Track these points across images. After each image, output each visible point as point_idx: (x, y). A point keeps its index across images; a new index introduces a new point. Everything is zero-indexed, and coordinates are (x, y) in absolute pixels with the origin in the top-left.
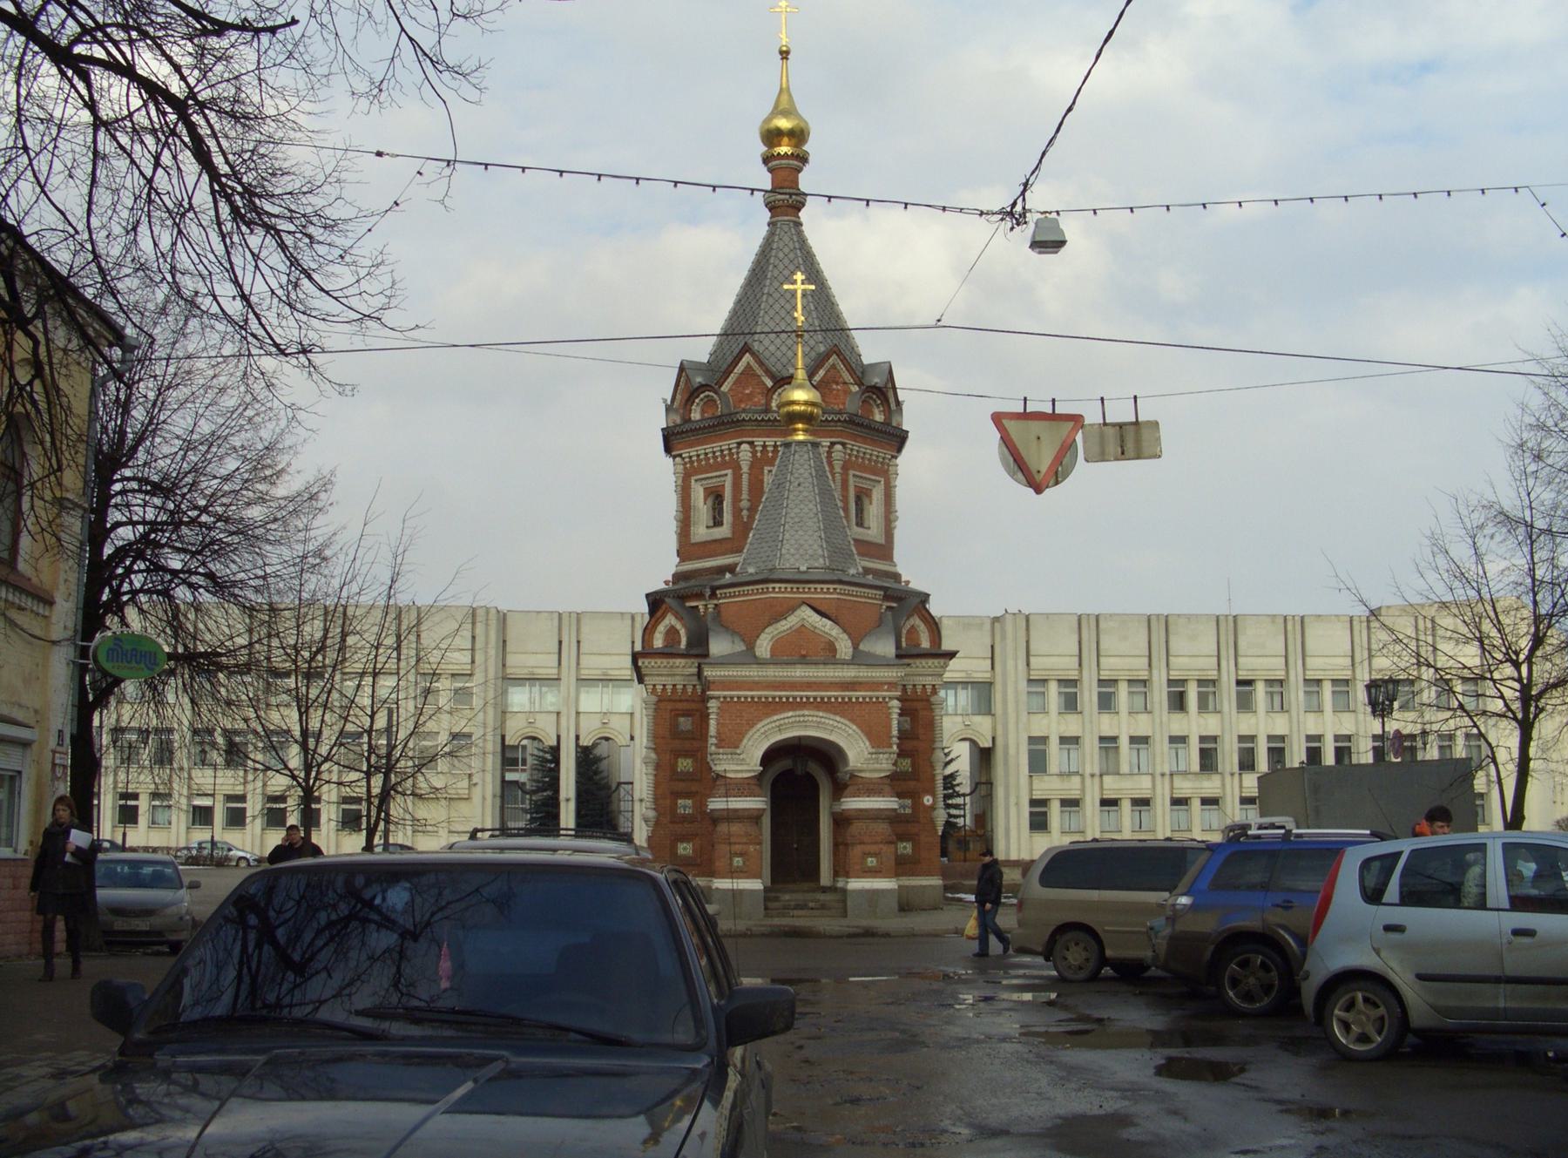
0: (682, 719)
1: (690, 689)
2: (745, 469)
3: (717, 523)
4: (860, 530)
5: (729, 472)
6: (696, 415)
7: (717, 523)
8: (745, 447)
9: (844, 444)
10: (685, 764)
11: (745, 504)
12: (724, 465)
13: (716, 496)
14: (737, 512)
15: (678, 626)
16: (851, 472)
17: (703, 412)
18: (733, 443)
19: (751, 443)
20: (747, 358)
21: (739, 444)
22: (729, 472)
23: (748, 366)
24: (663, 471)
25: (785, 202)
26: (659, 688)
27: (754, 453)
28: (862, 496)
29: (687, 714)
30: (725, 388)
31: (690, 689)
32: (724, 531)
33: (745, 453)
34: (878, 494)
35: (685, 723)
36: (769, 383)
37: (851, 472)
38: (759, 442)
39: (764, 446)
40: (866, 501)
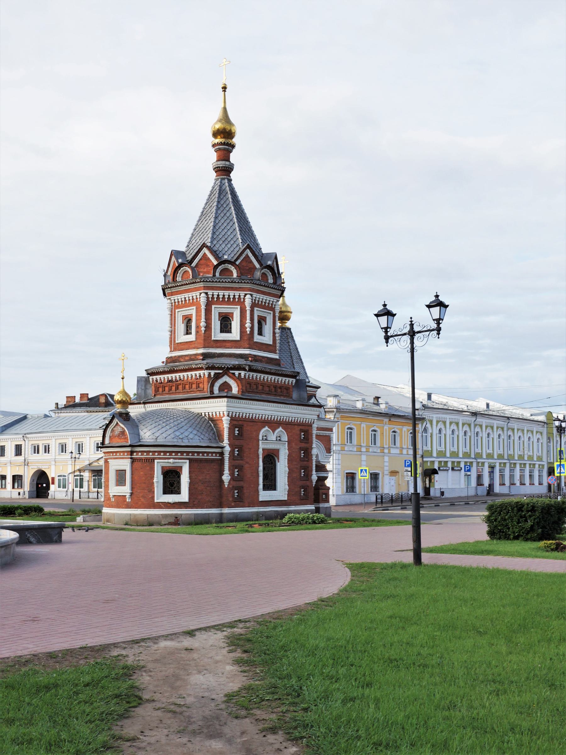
2: (203, 307)
5: (194, 307)
6: (179, 279)
7: (188, 332)
9: (251, 295)
11: (203, 324)
12: (192, 304)
13: (188, 320)
14: (198, 327)
16: (256, 309)
18: (198, 293)
19: (206, 293)
20: (205, 250)
21: (201, 293)
22: (194, 307)
24: (164, 305)
27: (208, 298)
28: (262, 321)
30: (194, 264)
32: (192, 337)
33: (203, 300)
36: (215, 263)
37: (256, 309)
38: (210, 293)
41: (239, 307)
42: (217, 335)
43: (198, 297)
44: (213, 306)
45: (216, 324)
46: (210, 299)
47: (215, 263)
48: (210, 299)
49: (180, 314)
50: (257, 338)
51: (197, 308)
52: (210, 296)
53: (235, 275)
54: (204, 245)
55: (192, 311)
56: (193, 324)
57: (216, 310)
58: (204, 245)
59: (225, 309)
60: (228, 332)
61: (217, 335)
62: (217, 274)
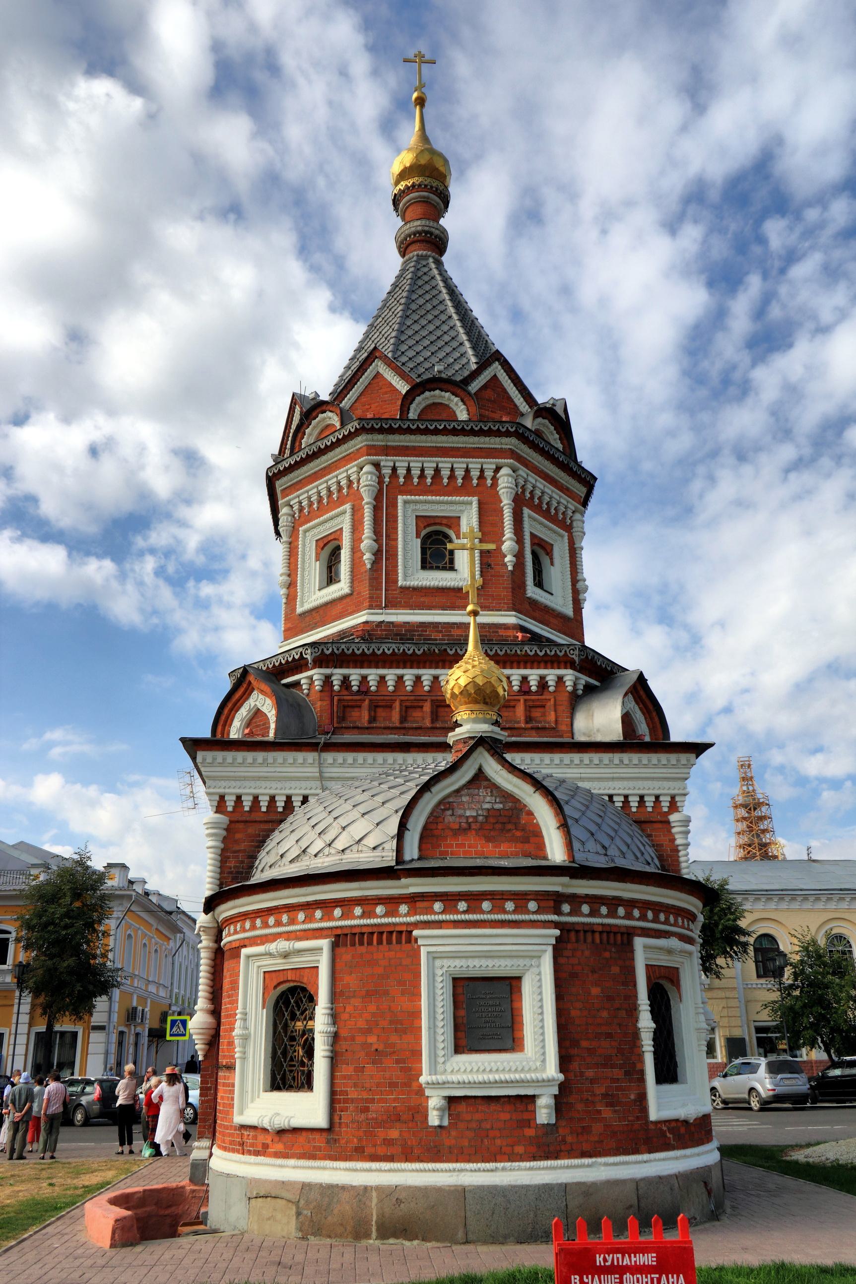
3: (331, 577)
4: (538, 590)
5: (347, 507)
7: (331, 577)
8: (367, 468)
34: (561, 550)
40: (545, 560)
41: (475, 500)
42: (412, 574)
44: (400, 499)
45: (408, 547)
47: (403, 387)
49: (309, 539)
50: (532, 591)
53: (462, 415)
55: (341, 521)
56: (345, 555)
57: (407, 510)
59: (436, 506)
60: (444, 569)
61: (412, 574)
62: (412, 415)
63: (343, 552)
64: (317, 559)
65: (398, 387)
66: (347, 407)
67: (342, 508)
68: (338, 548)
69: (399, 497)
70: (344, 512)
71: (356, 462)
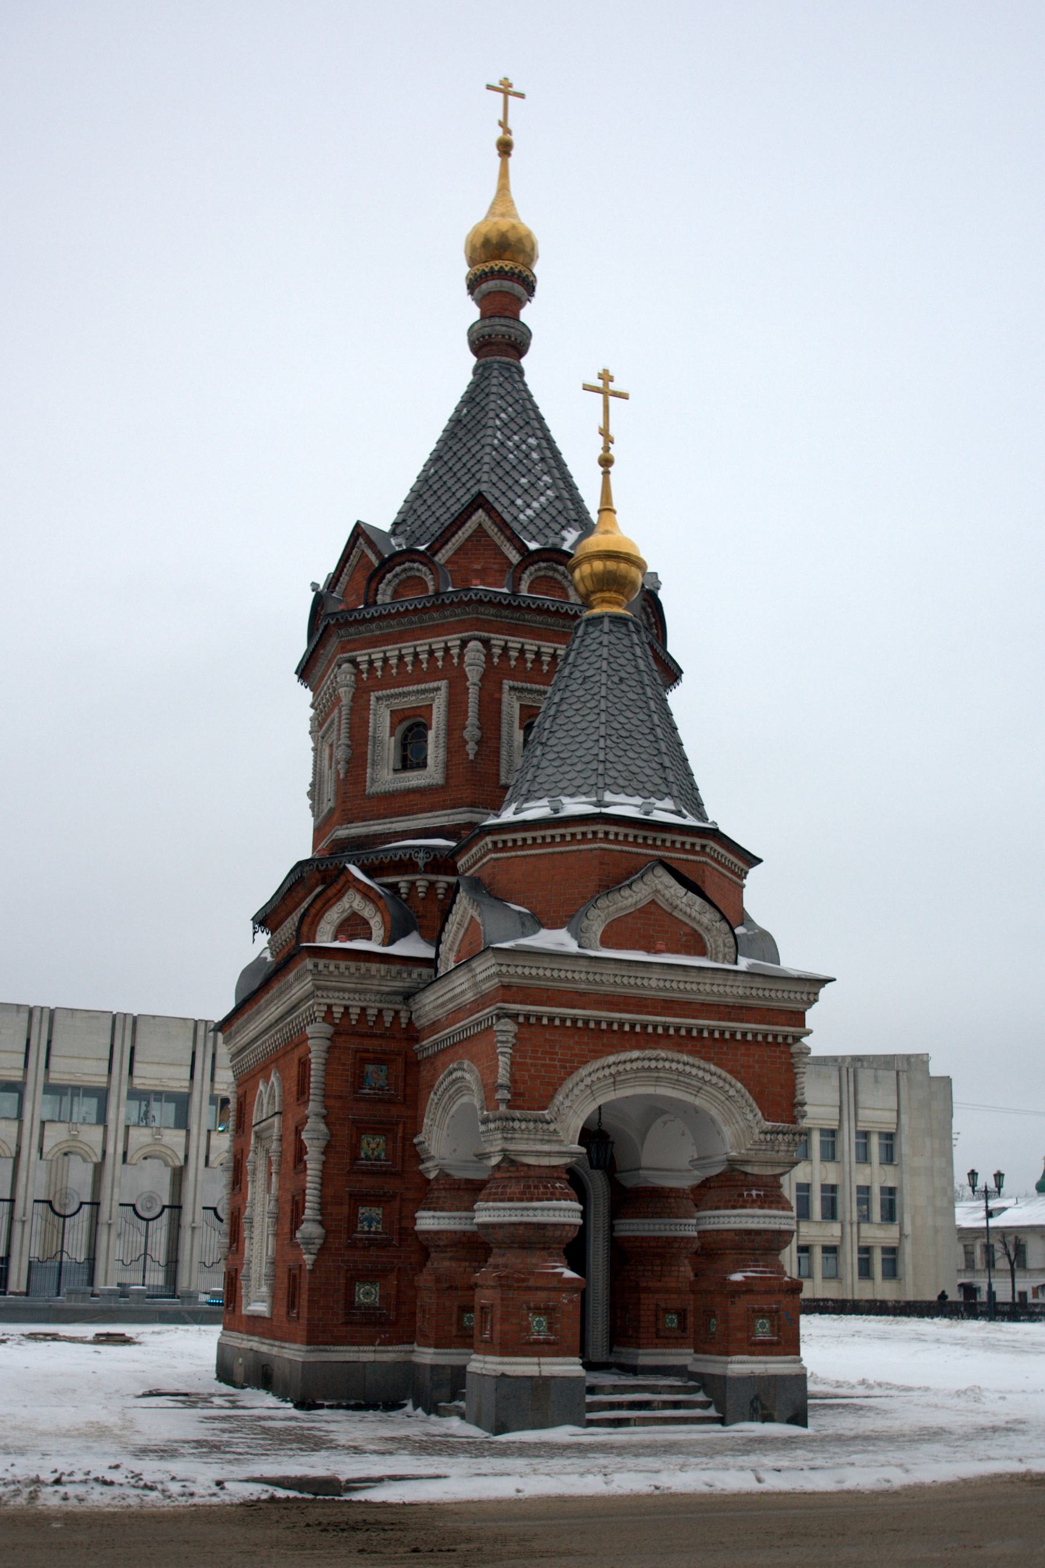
0: (370, 1068)
1: (388, 1018)
3: (411, 757)
5: (443, 684)
6: (384, 596)
10: (373, 1146)
11: (471, 731)
12: (434, 674)
15: (367, 911)
17: (396, 594)
18: (454, 641)
19: (486, 643)
20: (480, 515)
22: (443, 684)
23: (480, 530)
25: (499, 344)
26: (338, 1012)
27: (489, 656)
29: (380, 1059)
30: (441, 558)
31: (388, 1018)
35: (376, 1075)
38: (498, 640)
39: (505, 649)
43: (455, 651)
46: (496, 660)
48: (496, 660)
51: (450, 687)
52: (497, 651)
54: (479, 502)
58: (479, 502)
63: (431, 735)
64: (392, 734)
65: (510, 557)
66: (442, 562)
67: (435, 684)
68: (427, 727)
69: (505, 681)
70: (438, 689)
71: (460, 635)
